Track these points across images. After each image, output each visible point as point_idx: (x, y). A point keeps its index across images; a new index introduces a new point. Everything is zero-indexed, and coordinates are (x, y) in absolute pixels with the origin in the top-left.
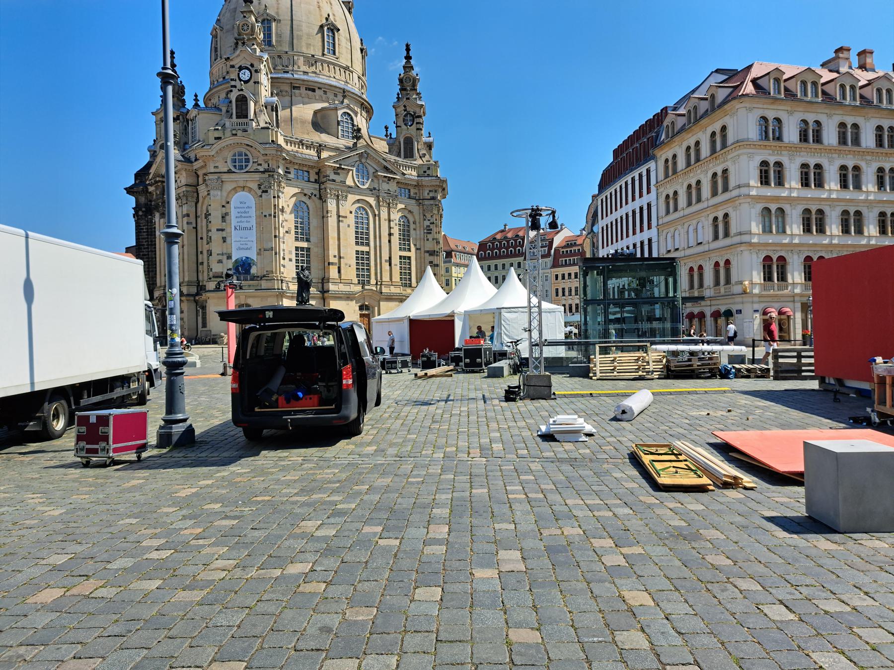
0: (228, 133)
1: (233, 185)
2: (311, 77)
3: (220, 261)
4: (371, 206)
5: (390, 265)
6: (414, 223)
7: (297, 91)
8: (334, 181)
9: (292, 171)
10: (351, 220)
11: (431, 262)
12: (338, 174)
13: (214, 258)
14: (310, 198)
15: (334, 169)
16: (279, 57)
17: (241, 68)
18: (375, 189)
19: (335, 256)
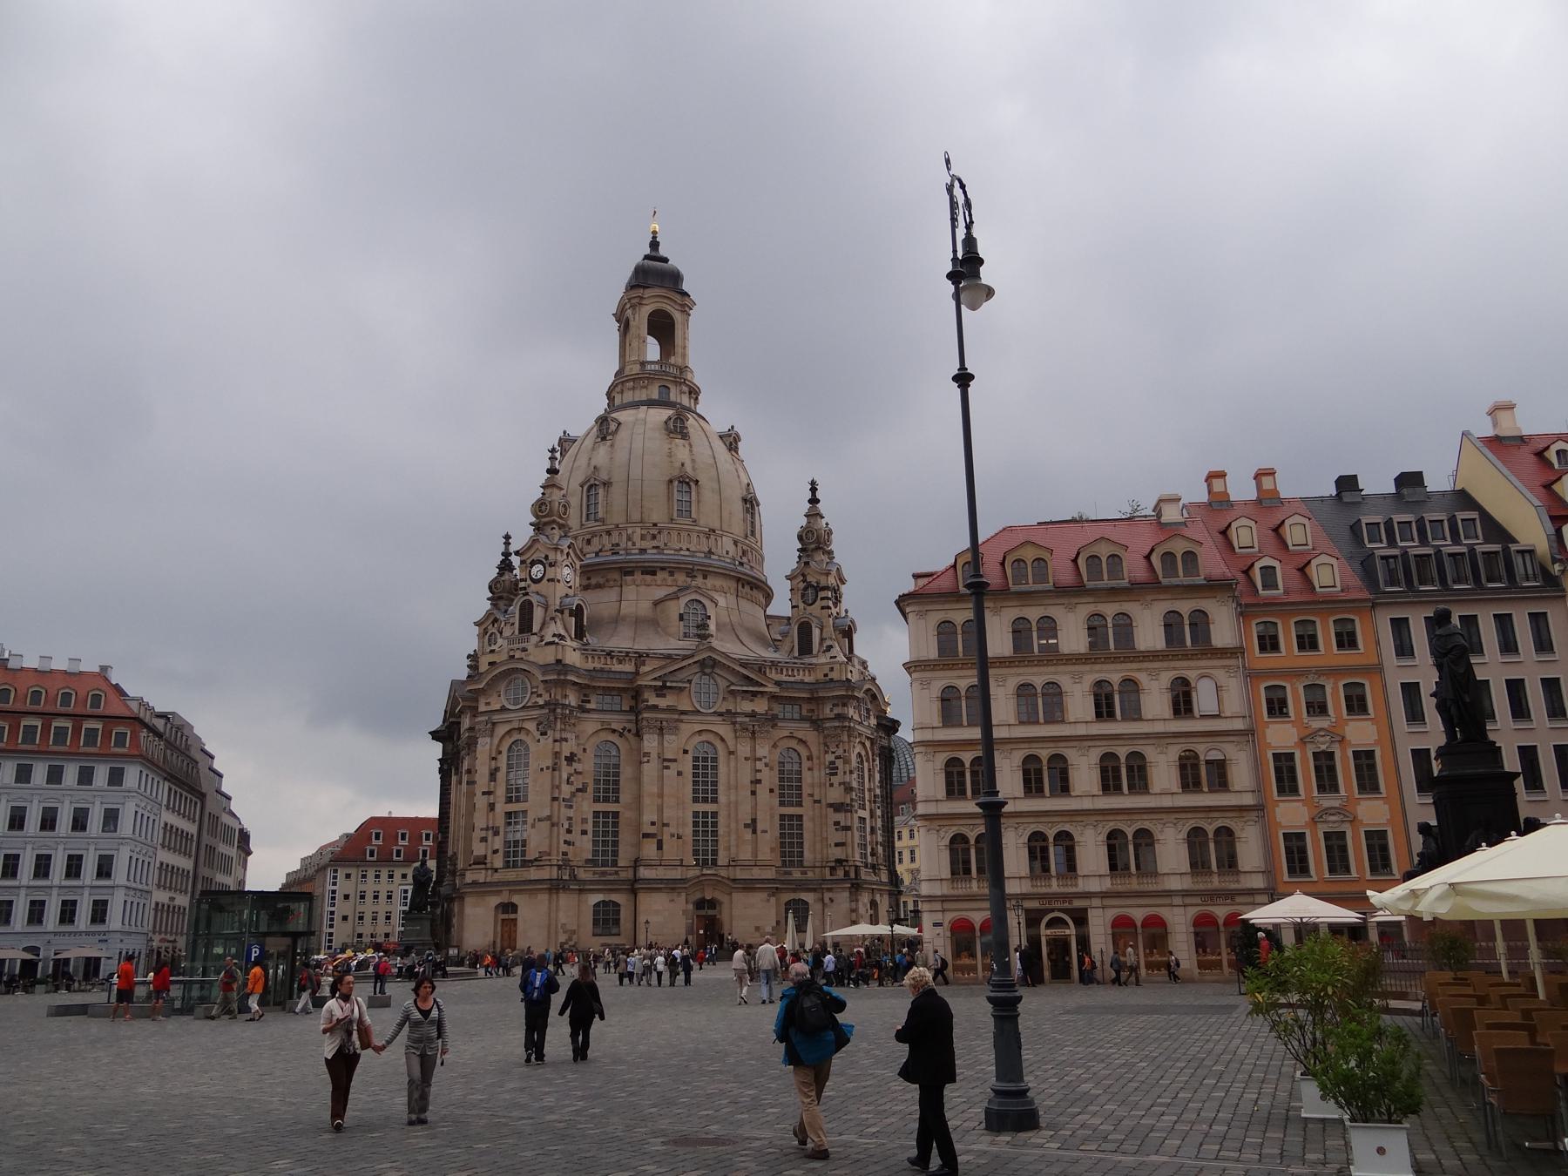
0: (505, 657)
1: (507, 727)
2: (651, 555)
3: (484, 840)
4: (723, 740)
5: (754, 832)
6: (810, 758)
7: (629, 578)
8: (655, 707)
9: (593, 698)
10: (687, 765)
11: (837, 823)
12: (664, 696)
13: (477, 834)
14: (621, 735)
15: (655, 688)
16: (609, 533)
17: (533, 563)
18: (729, 712)
19: (653, 824)
